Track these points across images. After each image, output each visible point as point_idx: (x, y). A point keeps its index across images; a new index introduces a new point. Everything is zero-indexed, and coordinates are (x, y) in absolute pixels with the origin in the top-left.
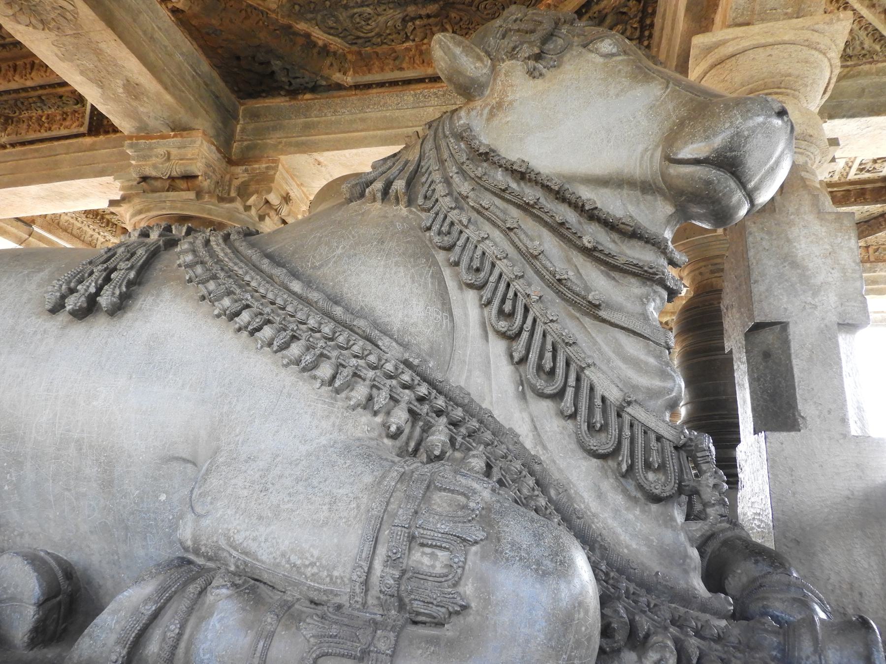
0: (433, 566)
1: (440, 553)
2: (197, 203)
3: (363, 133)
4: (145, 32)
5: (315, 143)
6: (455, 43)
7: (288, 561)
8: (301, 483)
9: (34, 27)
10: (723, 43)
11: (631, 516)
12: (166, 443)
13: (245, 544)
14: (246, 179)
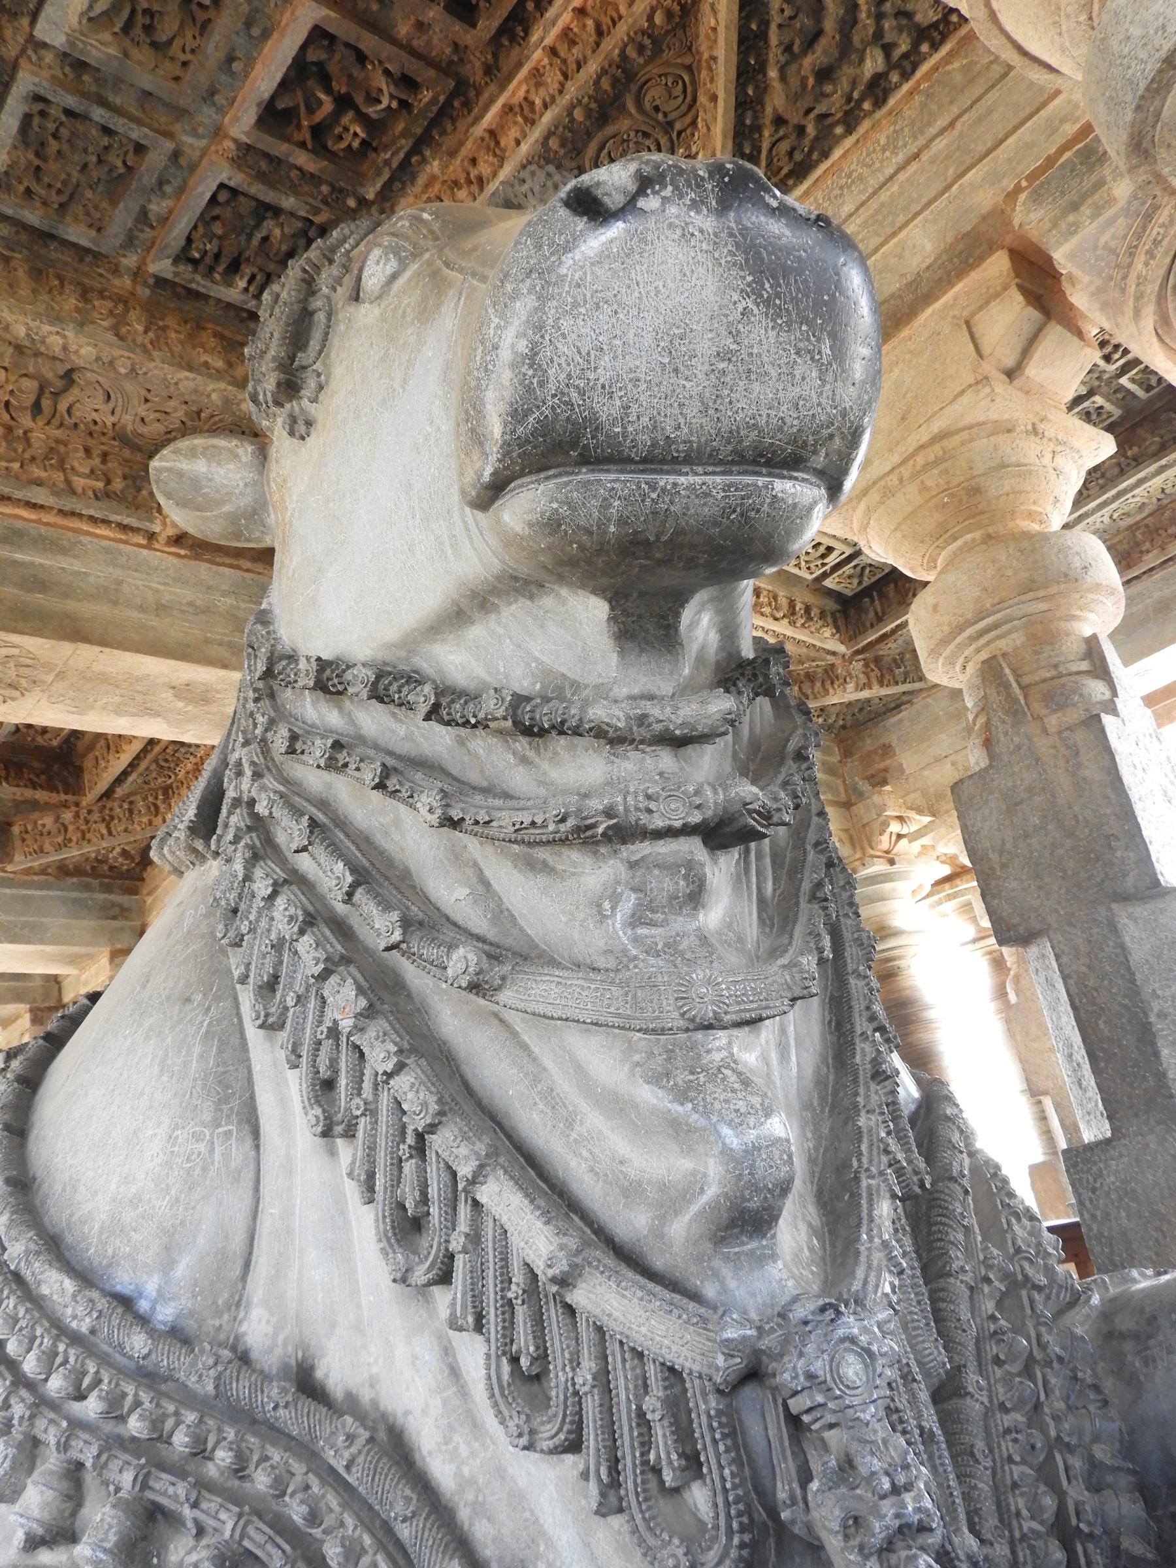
4: (142, 609)
9: (13, 699)
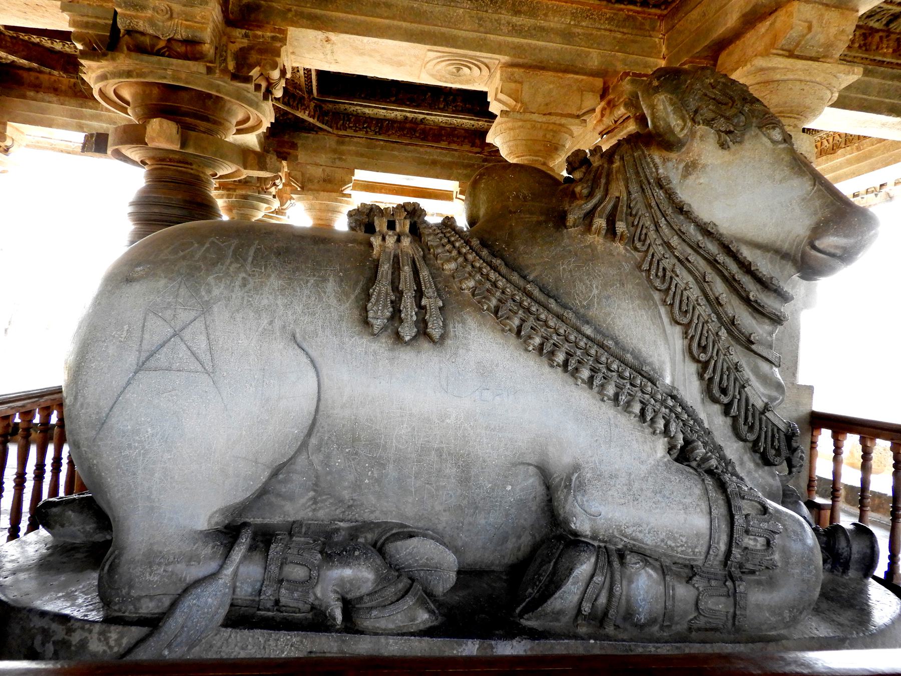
0: (756, 546)
1: (759, 539)
2: (206, 77)
3: (387, 21)
5: (332, 20)
6: (670, 103)
7: (666, 544)
8: (658, 495)
10: (774, 69)
11: (757, 475)
12: (516, 453)
13: (634, 535)
14: (245, 45)
